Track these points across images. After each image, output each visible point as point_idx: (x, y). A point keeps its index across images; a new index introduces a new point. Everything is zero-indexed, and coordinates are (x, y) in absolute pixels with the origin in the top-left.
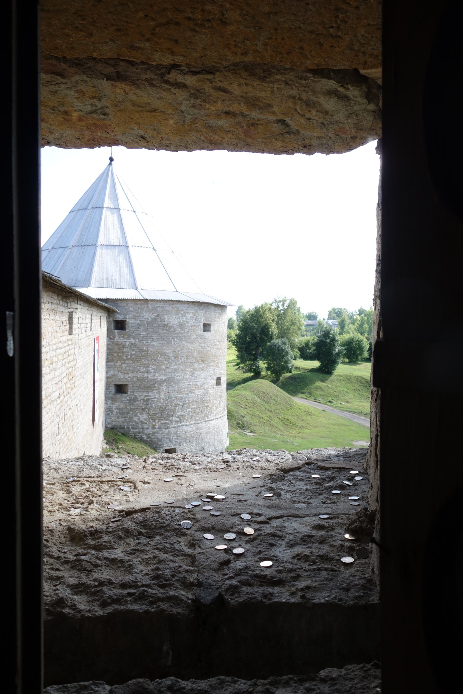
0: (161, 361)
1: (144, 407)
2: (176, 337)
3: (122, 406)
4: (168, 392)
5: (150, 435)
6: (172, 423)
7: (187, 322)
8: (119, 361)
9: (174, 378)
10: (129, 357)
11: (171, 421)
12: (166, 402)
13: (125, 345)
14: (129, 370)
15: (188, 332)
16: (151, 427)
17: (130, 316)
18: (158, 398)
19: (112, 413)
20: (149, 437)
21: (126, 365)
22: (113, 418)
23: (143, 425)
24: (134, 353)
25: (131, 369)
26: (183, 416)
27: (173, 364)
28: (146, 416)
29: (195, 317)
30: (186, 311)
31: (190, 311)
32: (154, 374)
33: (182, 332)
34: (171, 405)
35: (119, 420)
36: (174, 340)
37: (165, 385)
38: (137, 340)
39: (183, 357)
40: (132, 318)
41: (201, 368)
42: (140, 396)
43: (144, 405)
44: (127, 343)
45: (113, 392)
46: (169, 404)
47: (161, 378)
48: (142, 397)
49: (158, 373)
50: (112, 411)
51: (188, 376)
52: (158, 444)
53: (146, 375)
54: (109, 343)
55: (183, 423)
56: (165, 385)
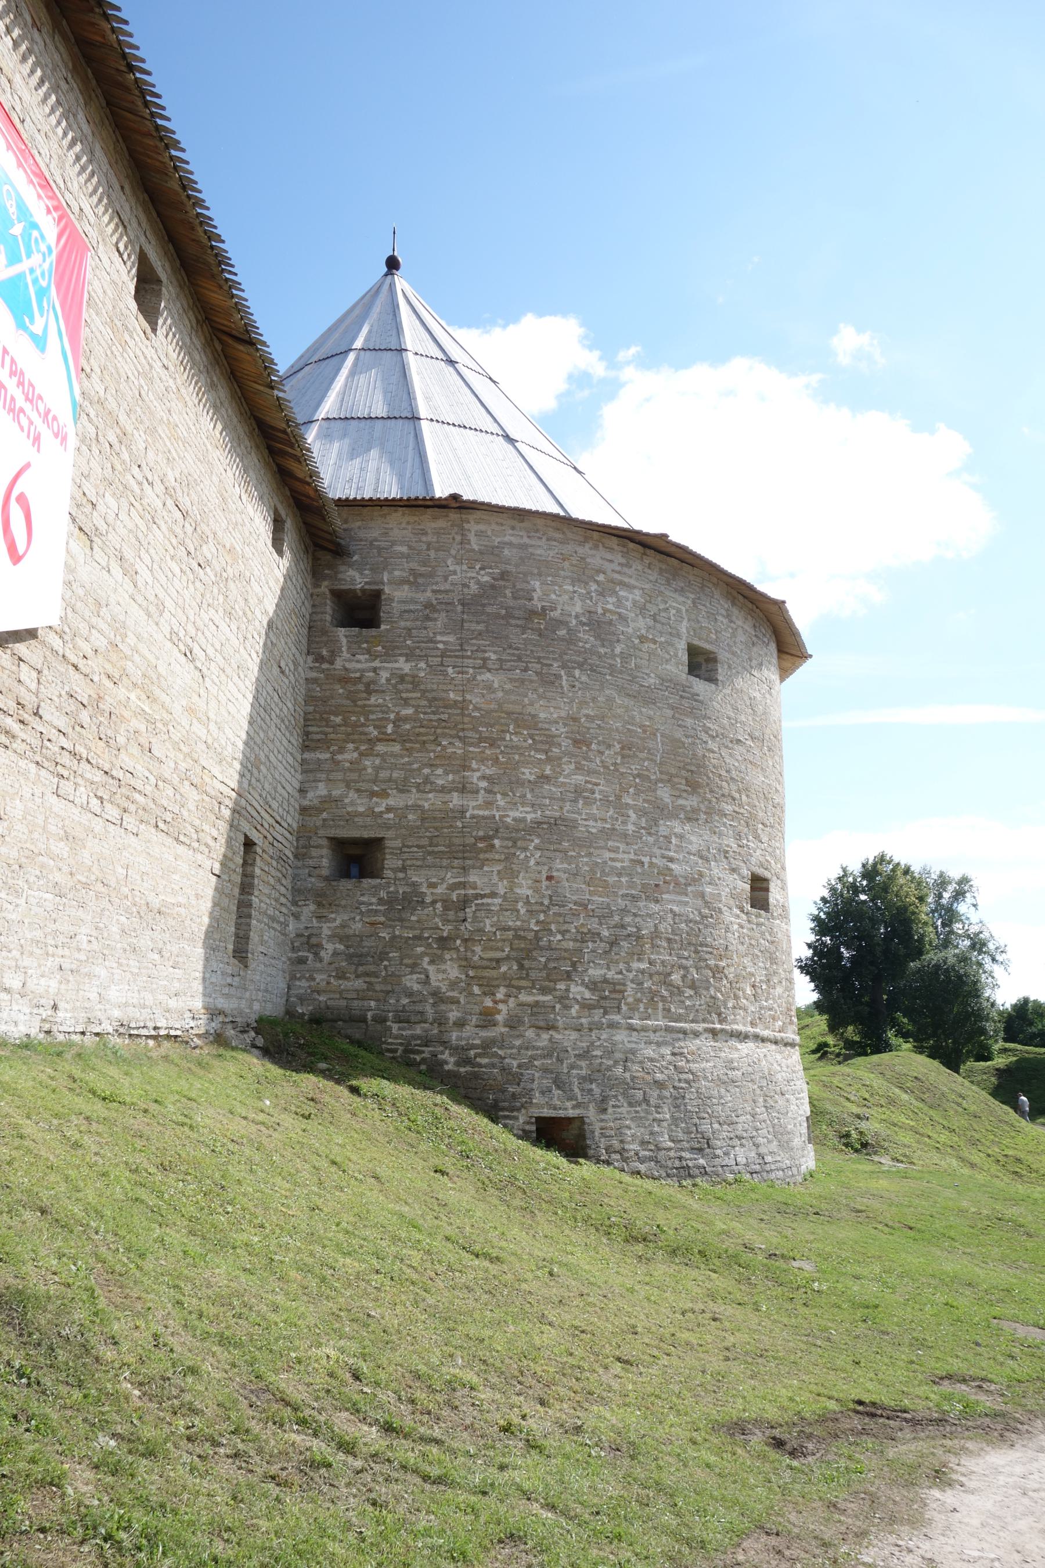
0: (517, 748)
1: (446, 930)
2: (580, 666)
3: (357, 927)
4: (549, 878)
5: (472, 1053)
6: (567, 1007)
7: (623, 618)
8: (351, 746)
9: (573, 825)
10: (390, 729)
11: (564, 999)
12: (542, 917)
13: (374, 682)
14: (390, 780)
15: (625, 657)
16: (474, 1020)
17: (397, 573)
18: (504, 897)
19: (316, 954)
20: (467, 1061)
21: (377, 762)
22: (319, 977)
23: (443, 1007)
24: (410, 711)
25: (395, 775)
26: (617, 988)
27: (569, 768)
28: (453, 971)
29: (653, 609)
30: (617, 576)
31: (633, 582)
33: (602, 650)
34: (563, 933)
35: (345, 984)
36: (570, 675)
37: (536, 848)
38: (422, 665)
39: (609, 747)
40: (403, 582)
41: (682, 808)
42: (432, 885)
43: (446, 921)
44: (384, 675)
45: (325, 872)
46: (553, 927)
47: (517, 814)
48: (439, 890)
49: (504, 795)
50: (315, 948)
52: (503, 1091)
53: (456, 800)
54: (314, 675)
56: (536, 848)
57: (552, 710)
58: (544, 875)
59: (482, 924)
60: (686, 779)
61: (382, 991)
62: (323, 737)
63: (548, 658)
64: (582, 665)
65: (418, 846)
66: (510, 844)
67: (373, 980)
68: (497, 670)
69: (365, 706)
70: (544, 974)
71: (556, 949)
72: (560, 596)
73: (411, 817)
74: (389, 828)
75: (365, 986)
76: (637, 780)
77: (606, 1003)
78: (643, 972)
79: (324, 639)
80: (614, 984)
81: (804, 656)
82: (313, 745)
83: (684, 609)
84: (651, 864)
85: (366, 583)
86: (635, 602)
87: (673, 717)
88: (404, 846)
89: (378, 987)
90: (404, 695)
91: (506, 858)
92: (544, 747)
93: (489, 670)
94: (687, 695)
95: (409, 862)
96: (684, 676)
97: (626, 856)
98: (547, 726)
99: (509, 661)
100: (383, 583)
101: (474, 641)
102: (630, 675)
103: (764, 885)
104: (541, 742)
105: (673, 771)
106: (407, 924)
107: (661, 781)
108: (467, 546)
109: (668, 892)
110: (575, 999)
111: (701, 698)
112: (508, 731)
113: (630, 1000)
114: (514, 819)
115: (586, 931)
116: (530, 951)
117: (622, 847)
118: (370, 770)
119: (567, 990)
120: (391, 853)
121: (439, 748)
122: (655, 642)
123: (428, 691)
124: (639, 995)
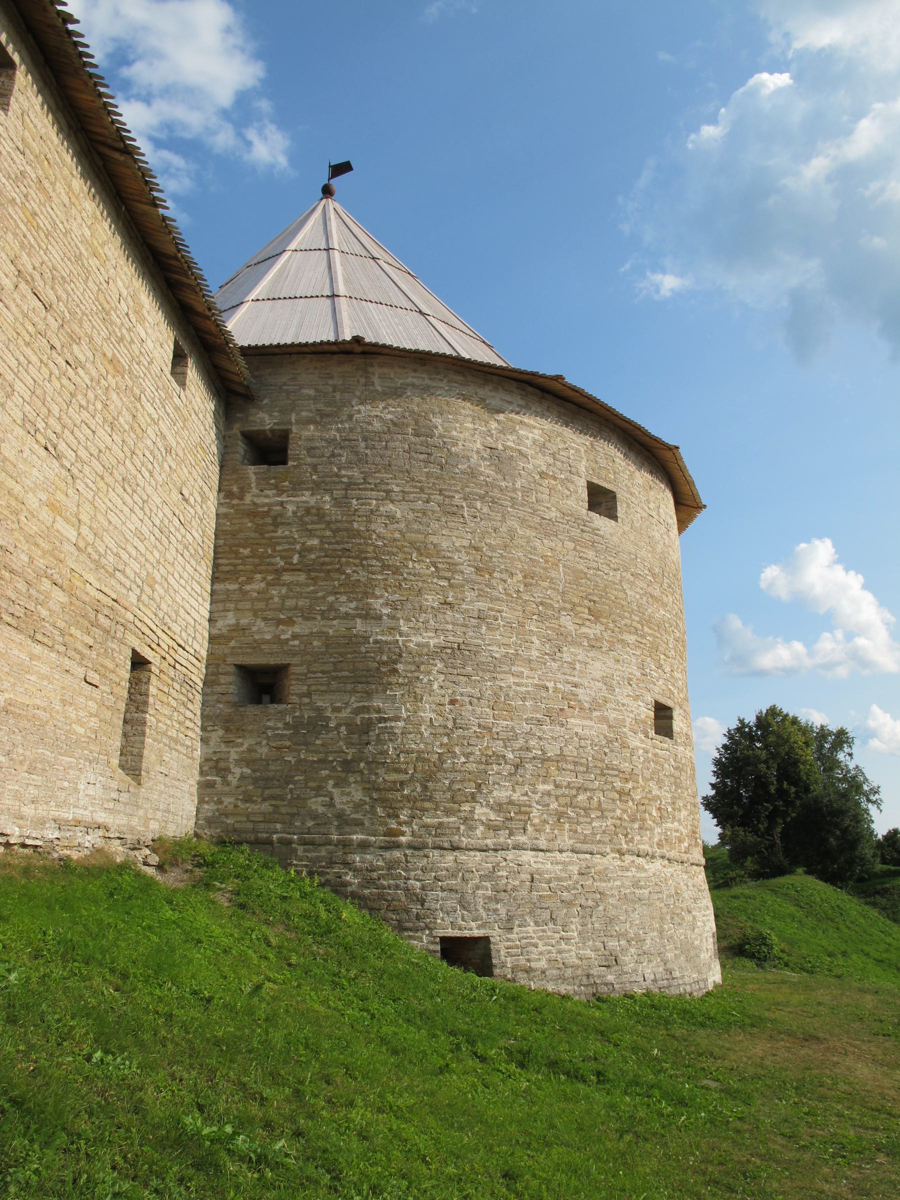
0: (419, 575)
1: (350, 753)
2: (482, 498)
3: (264, 751)
4: (453, 702)
5: (375, 875)
6: (472, 828)
8: (258, 576)
10: (296, 559)
12: (445, 740)
13: (281, 515)
14: (296, 608)
15: (526, 491)
17: (304, 414)
18: (407, 720)
20: (369, 882)
21: (284, 590)
22: (227, 800)
24: (315, 542)
25: (301, 603)
26: (523, 810)
27: (469, 595)
28: (358, 795)
32: (392, 623)
33: (503, 484)
34: (467, 755)
35: (252, 808)
37: (439, 672)
38: (327, 498)
40: (309, 421)
42: (337, 710)
43: (350, 744)
44: (291, 508)
45: (235, 699)
46: (457, 750)
47: (420, 639)
48: (345, 714)
51: (535, 653)
52: (407, 911)
53: (360, 626)
54: (224, 510)
55: (522, 839)
57: (454, 538)
58: (447, 699)
59: (385, 747)
60: (589, 609)
61: (287, 814)
62: (232, 568)
63: (450, 490)
64: (483, 498)
65: (323, 672)
66: (413, 668)
67: (279, 803)
68: (399, 501)
69: (272, 538)
70: (448, 795)
71: (460, 771)
72: (461, 432)
73: (315, 643)
74: (294, 655)
75: (271, 809)
76: (540, 608)
77: (513, 824)
78: (548, 794)
79: (235, 476)
80: (520, 806)
81: (700, 507)
82: (222, 576)
83: (583, 450)
84: (556, 690)
85: (275, 424)
86: (534, 442)
87: (575, 549)
88: (309, 672)
89: (283, 810)
90: (310, 527)
92: (449, 574)
93: (392, 502)
94: (587, 529)
95: (313, 688)
96: (584, 511)
97: (530, 681)
98: (450, 555)
100: (291, 424)
101: (377, 475)
103: (668, 713)
104: (444, 570)
105: (576, 600)
106: (312, 748)
107: (564, 609)
108: (371, 388)
109: (573, 717)
110: (480, 820)
111: (601, 533)
112: (411, 559)
113: (536, 821)
114: (418, 645)
115: (490, 753)
117: (526, 672)
118: (276, 599)
119: (472, 812)
120: (298, 679)
121: (344, 577)
122: (555, 479)
124: (545, 816)
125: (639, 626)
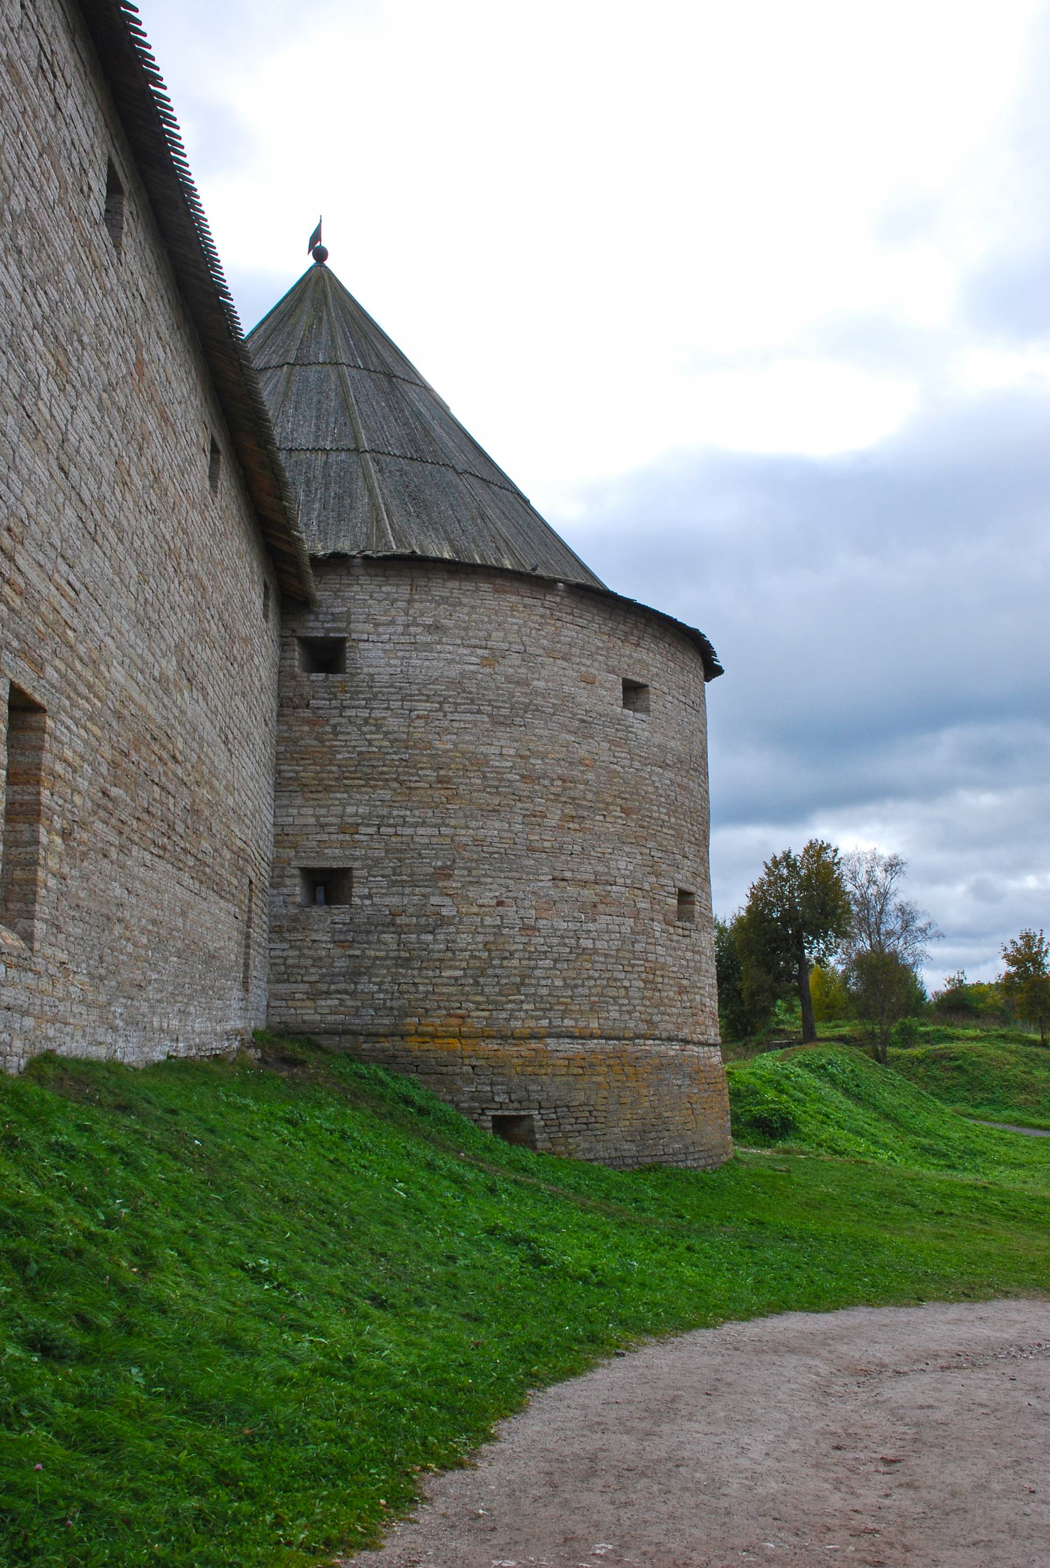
25: (360, 810)
60: (621, 806)
61: (353, 1007)
65: (383, 876)
67: (344, 996)
70: (497, 989)
90: (368, 737)
91: (463, 886)
95: (375, 890)
99: (464, 704)
101: (431, 686)
102: (571, 713)
104: (492, 778)
105: (610, 800)
116: (485, 969)
120: (359, 882)
123: (390, 733)
125: (666, 818)
